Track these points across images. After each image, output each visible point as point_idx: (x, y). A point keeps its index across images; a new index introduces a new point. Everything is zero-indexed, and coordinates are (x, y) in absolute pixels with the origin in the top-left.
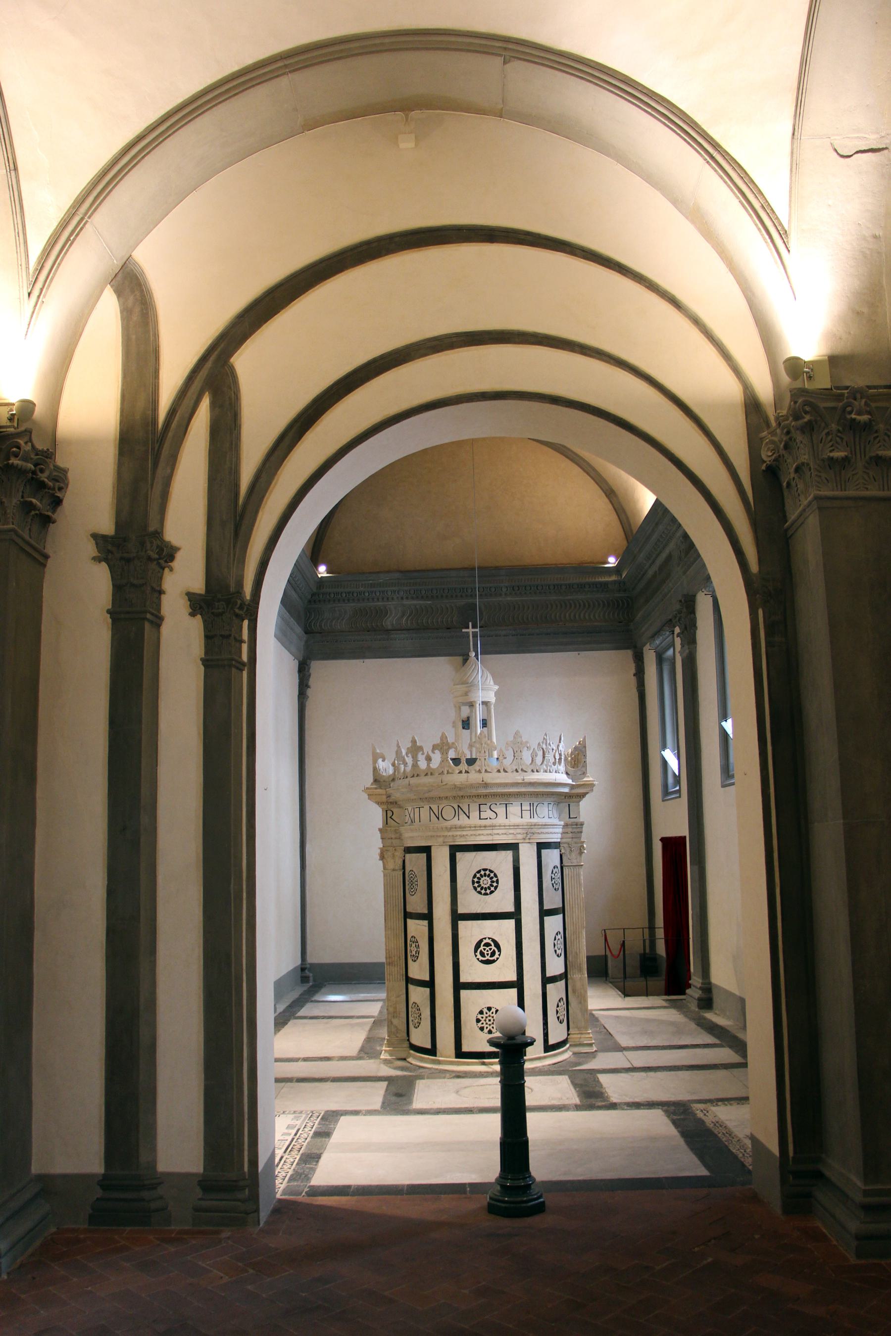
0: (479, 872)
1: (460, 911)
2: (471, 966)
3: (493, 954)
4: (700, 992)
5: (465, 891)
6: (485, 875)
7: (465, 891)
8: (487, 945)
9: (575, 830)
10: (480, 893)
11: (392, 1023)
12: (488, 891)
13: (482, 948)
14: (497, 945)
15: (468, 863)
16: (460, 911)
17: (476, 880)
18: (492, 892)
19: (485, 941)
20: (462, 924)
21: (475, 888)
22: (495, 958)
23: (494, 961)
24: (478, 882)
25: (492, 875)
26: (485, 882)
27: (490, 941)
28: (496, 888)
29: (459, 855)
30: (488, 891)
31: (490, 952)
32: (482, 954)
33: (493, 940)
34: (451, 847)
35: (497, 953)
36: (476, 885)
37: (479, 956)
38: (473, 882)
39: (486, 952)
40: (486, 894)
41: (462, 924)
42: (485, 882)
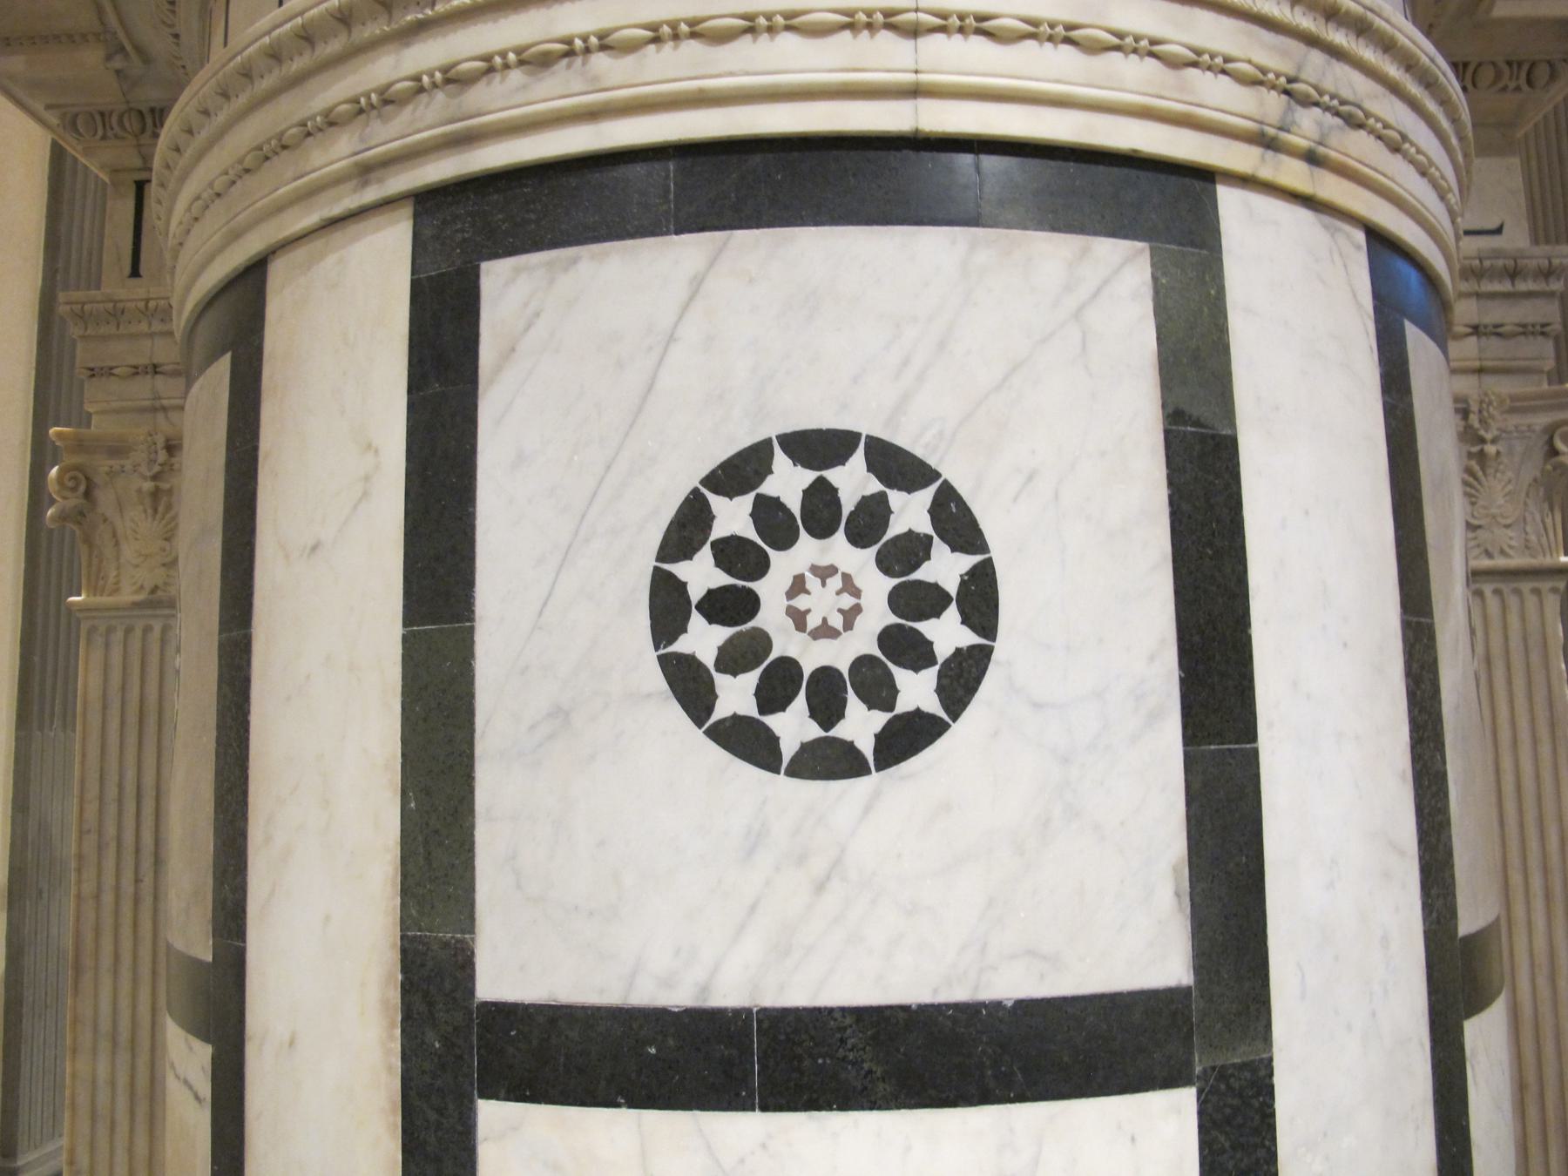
0: (741, 472)
1: (497, 980)
5: (561, 715)
6: (821, 511)
7: (561, 715)
9: (1497, 313)
10: (747, 741)
12: (860, 725)
15: (632, 379)
16: (497, 980)
17: (701, 574)
18: (907, 738)
21: (690, 686)
24: (730, 606)
25: (910, 512)
26: (826, 601)
28: (963, 678)
29: (509, 288)
30: (860, 725)
34: (427, 201)
36: (703, 640)
38: (668, 607)
40: (830, 761)
42: (826, 601)
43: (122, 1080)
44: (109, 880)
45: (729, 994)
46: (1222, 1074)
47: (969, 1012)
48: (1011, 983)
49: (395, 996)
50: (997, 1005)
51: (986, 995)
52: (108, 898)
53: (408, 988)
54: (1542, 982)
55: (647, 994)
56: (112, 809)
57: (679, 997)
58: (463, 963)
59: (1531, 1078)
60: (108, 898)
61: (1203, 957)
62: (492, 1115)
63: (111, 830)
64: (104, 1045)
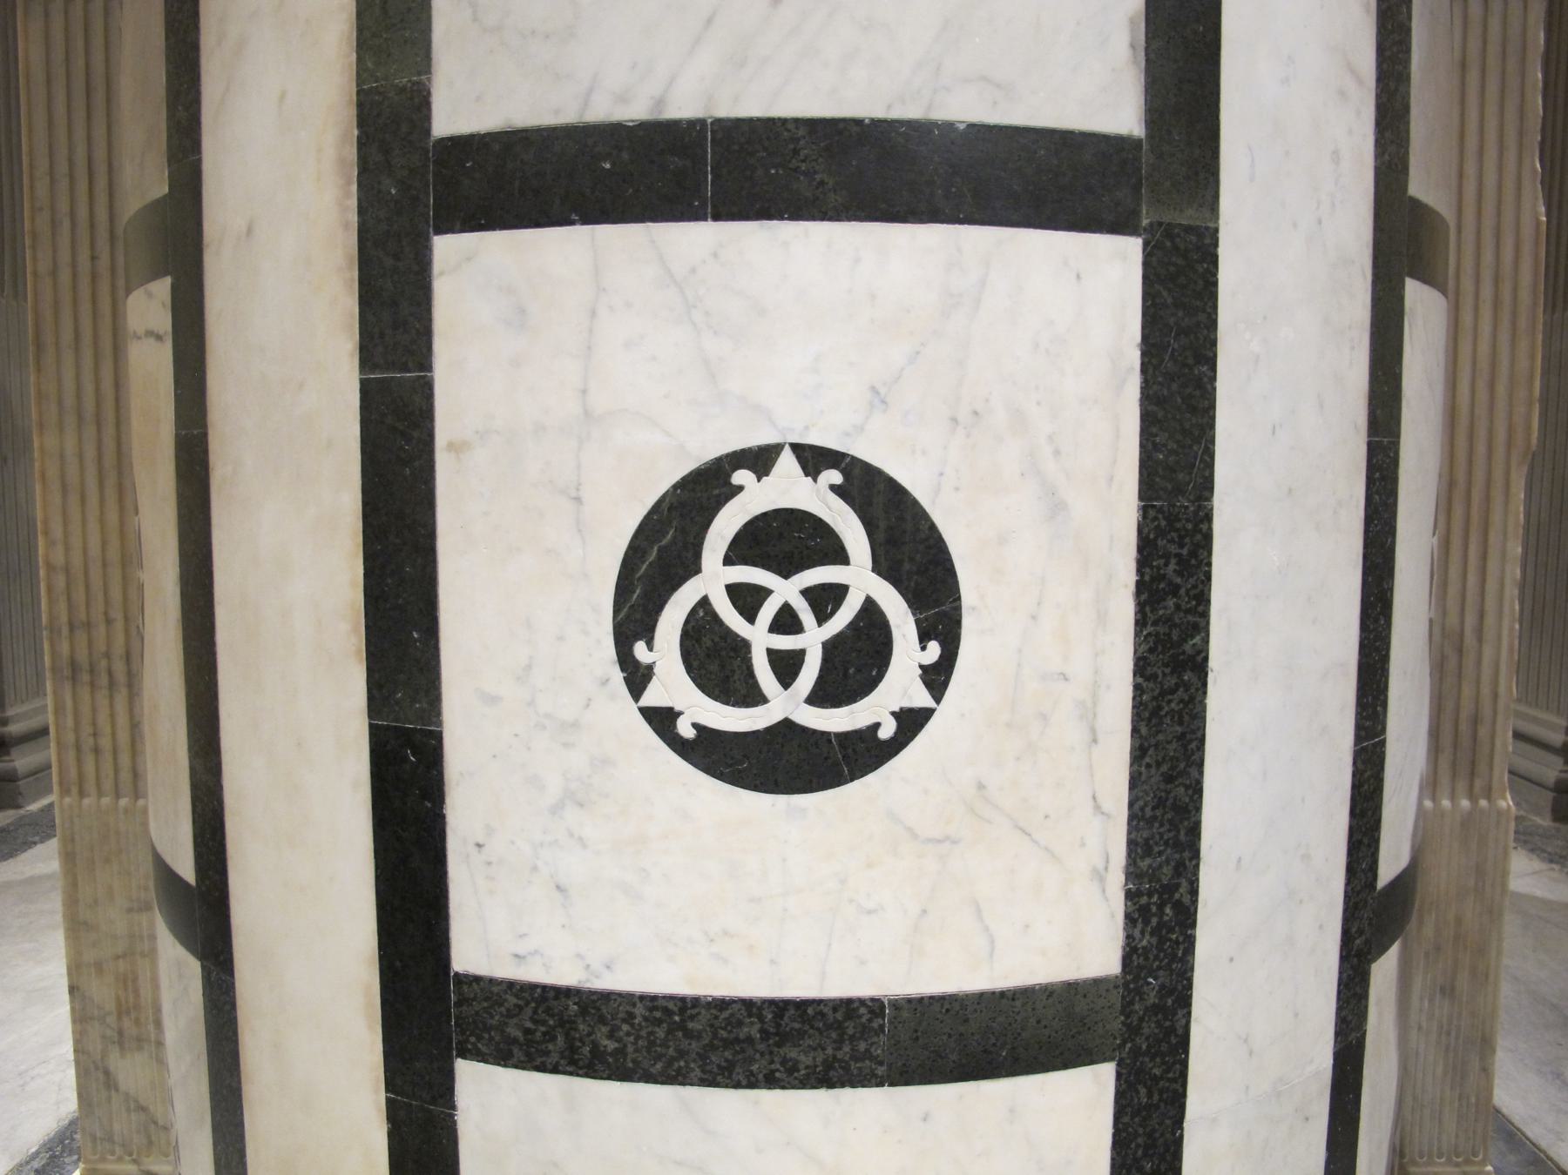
2: (576, 798)
3: (857, 661)
4: (1558, 762)
8: (785, 540)
11: (110, 1082)
13: (713, 578)
14: (918, 558)
19: (755, 497)
20: (473, 271)
22: (874, 711)
23: (862, 754)
27: (816, 497)
31: (813, 639)
32: (717, 661)
33: (869, 489)
35: (909, 651)
37: (672, 684)
39: (760, 637)
41: (473, 271)
43: (90, 453)
44: (65, 256)
45: (683, 107)
46: (1169, 231)
47: (919, 130)
48: (964, 106)
49: (352, 153)
50: (949, 126)
51: (941, 114)
52: (65, 276)
53: (363, 120)
54: (1482, 385)
55: (602, 110)
56: (63, 184)
57: (635, 111)
58: (421, 103)
59: (1461, 476)
60: (65, 276)
61: (1154, 114)
62: (447, 248)
63: (63, 206)
64: (70, 420)
